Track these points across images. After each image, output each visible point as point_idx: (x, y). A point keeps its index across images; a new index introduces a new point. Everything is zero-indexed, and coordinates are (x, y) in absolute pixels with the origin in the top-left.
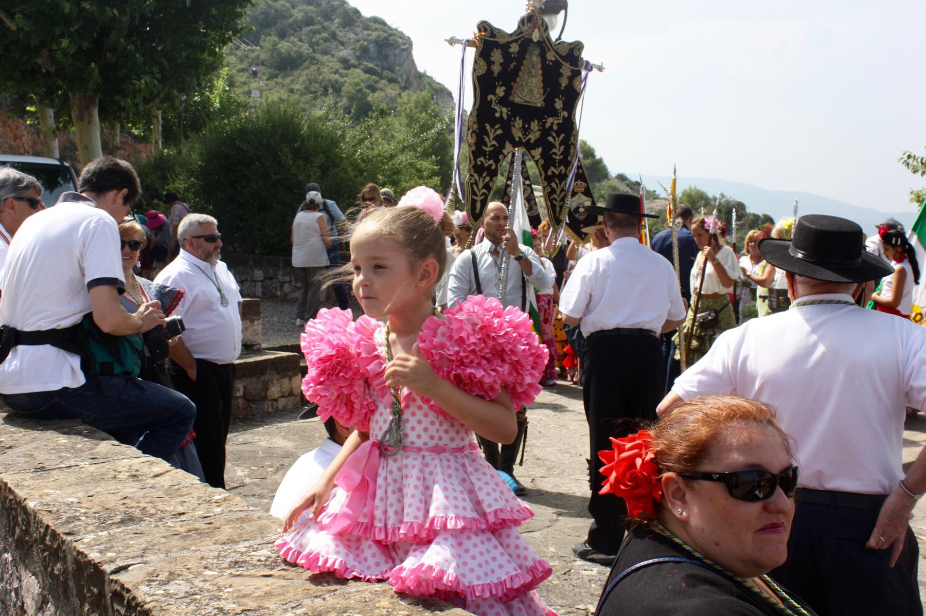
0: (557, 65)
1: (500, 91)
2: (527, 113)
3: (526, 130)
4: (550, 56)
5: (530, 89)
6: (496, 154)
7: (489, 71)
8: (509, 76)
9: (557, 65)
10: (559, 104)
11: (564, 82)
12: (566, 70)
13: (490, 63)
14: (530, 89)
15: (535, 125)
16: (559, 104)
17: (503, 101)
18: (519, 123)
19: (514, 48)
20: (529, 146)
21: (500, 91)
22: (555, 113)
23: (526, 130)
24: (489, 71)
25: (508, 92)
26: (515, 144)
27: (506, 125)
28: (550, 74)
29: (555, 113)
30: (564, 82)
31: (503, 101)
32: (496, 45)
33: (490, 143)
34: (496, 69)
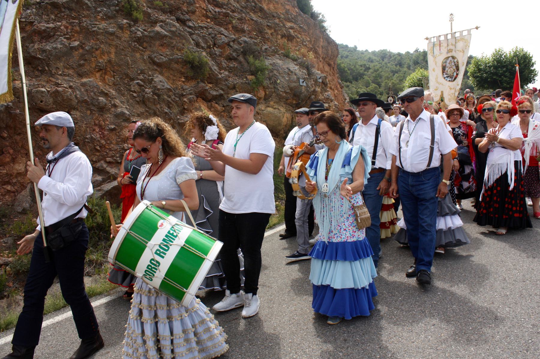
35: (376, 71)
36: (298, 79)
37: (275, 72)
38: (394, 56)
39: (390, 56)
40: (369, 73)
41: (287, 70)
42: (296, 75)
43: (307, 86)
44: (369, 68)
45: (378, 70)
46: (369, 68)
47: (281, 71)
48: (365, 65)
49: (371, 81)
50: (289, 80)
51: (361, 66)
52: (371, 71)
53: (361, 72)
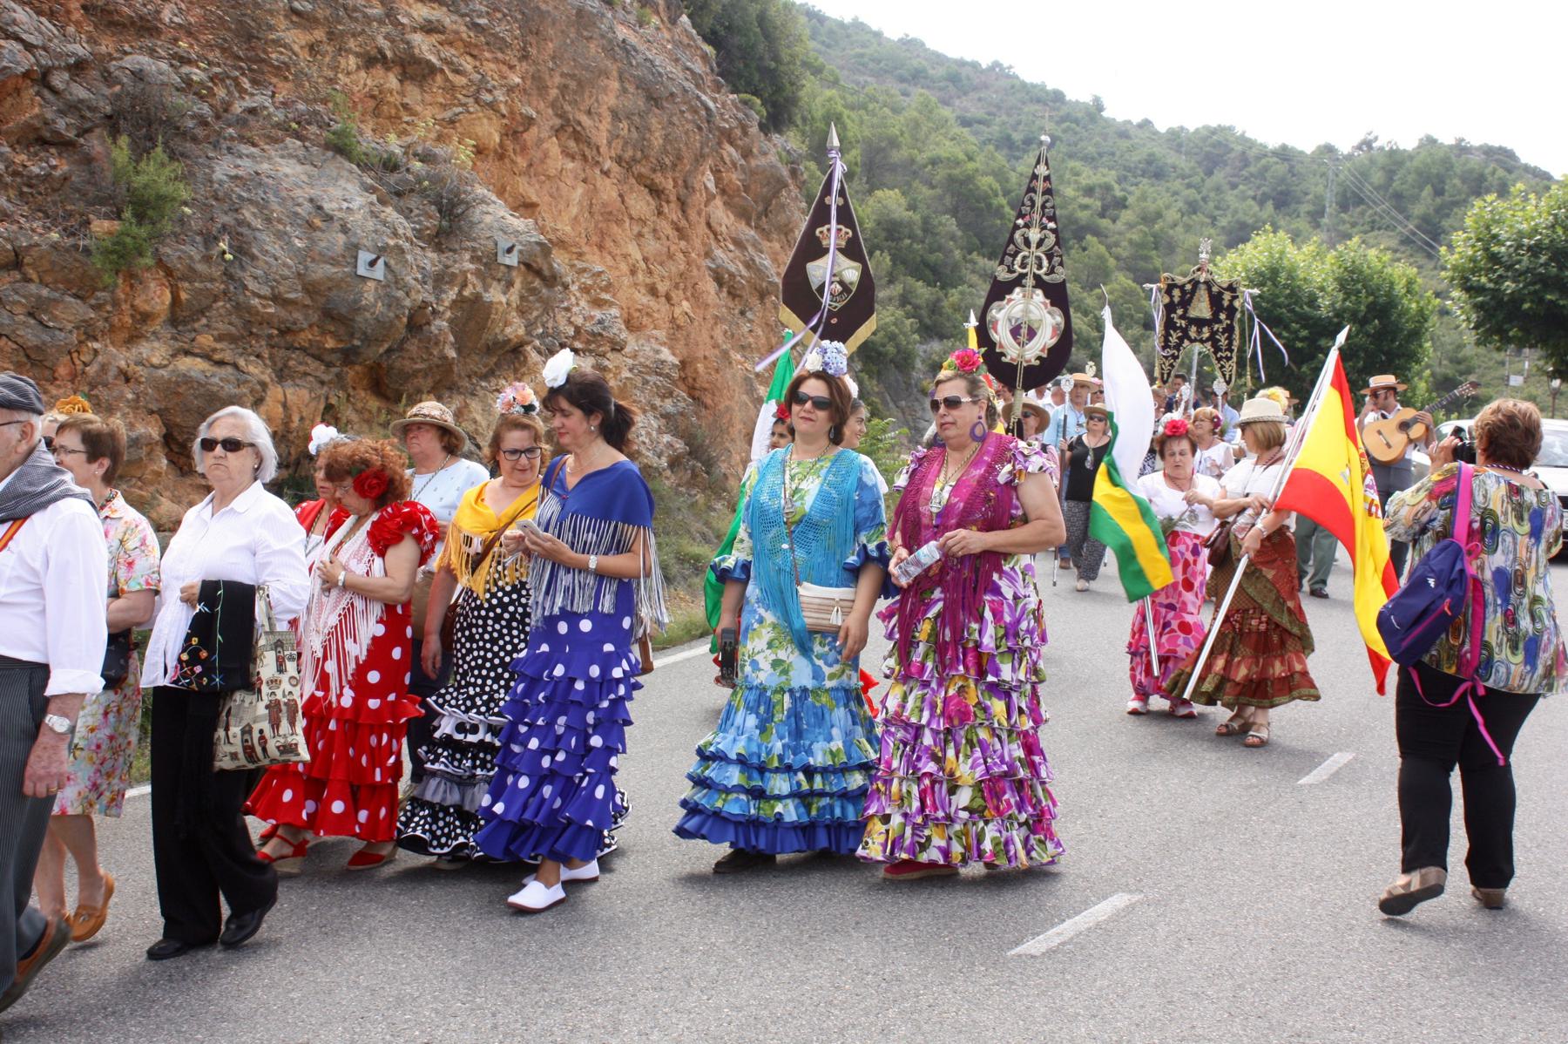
0: (1220, 294)
1: (1180, 312)
2: (1200, 323)
3: (1199, 332)
4: (1215, 289)
5: (1201, 308)
6: (1178, 347)
7: (1172, 301)
8: (1186, 302)
9: (1220, 294)
10: (1222, 316)
11: (1226, 303)
12: (1227, 296)
13: (1171, 297)
14: (1201, 308)
15: (1205, 329)
16: (1222, 316)
17: (1182, 317)
18: (1194, 328)
19: (1188, 287)
20: (1202, 341)
21: (1180, 312)
22: (1220, 322)
23: (1199, 332)
24: (1172, 301)
25: (1186, 311)
26: (1192, 341)
27: (1185, 331)
28: (1216, 300)
29: (1220, 322)
30: (1226, 303)
31: (1182, 317)
32: (1175, 286)
33: (1173, 340)
34: (1176, 300)
35: (1148, 219)
36: (353, 249)
37: (248, 213)
38: (1258, 158)
39: (1245, 161)
40: (1119, 226)
41: (305, 210)
42: (345, 230)
43: (395, 280)
44: (1121, 204)
45: (1159, 215)
46: (1121, 204)
47: (277, 210)
48: (1108, 188)
49: (1112, 262)
50: (309, 249)
51: (1089, 191)
52: (1127, 215)
53: (1083, 216)
